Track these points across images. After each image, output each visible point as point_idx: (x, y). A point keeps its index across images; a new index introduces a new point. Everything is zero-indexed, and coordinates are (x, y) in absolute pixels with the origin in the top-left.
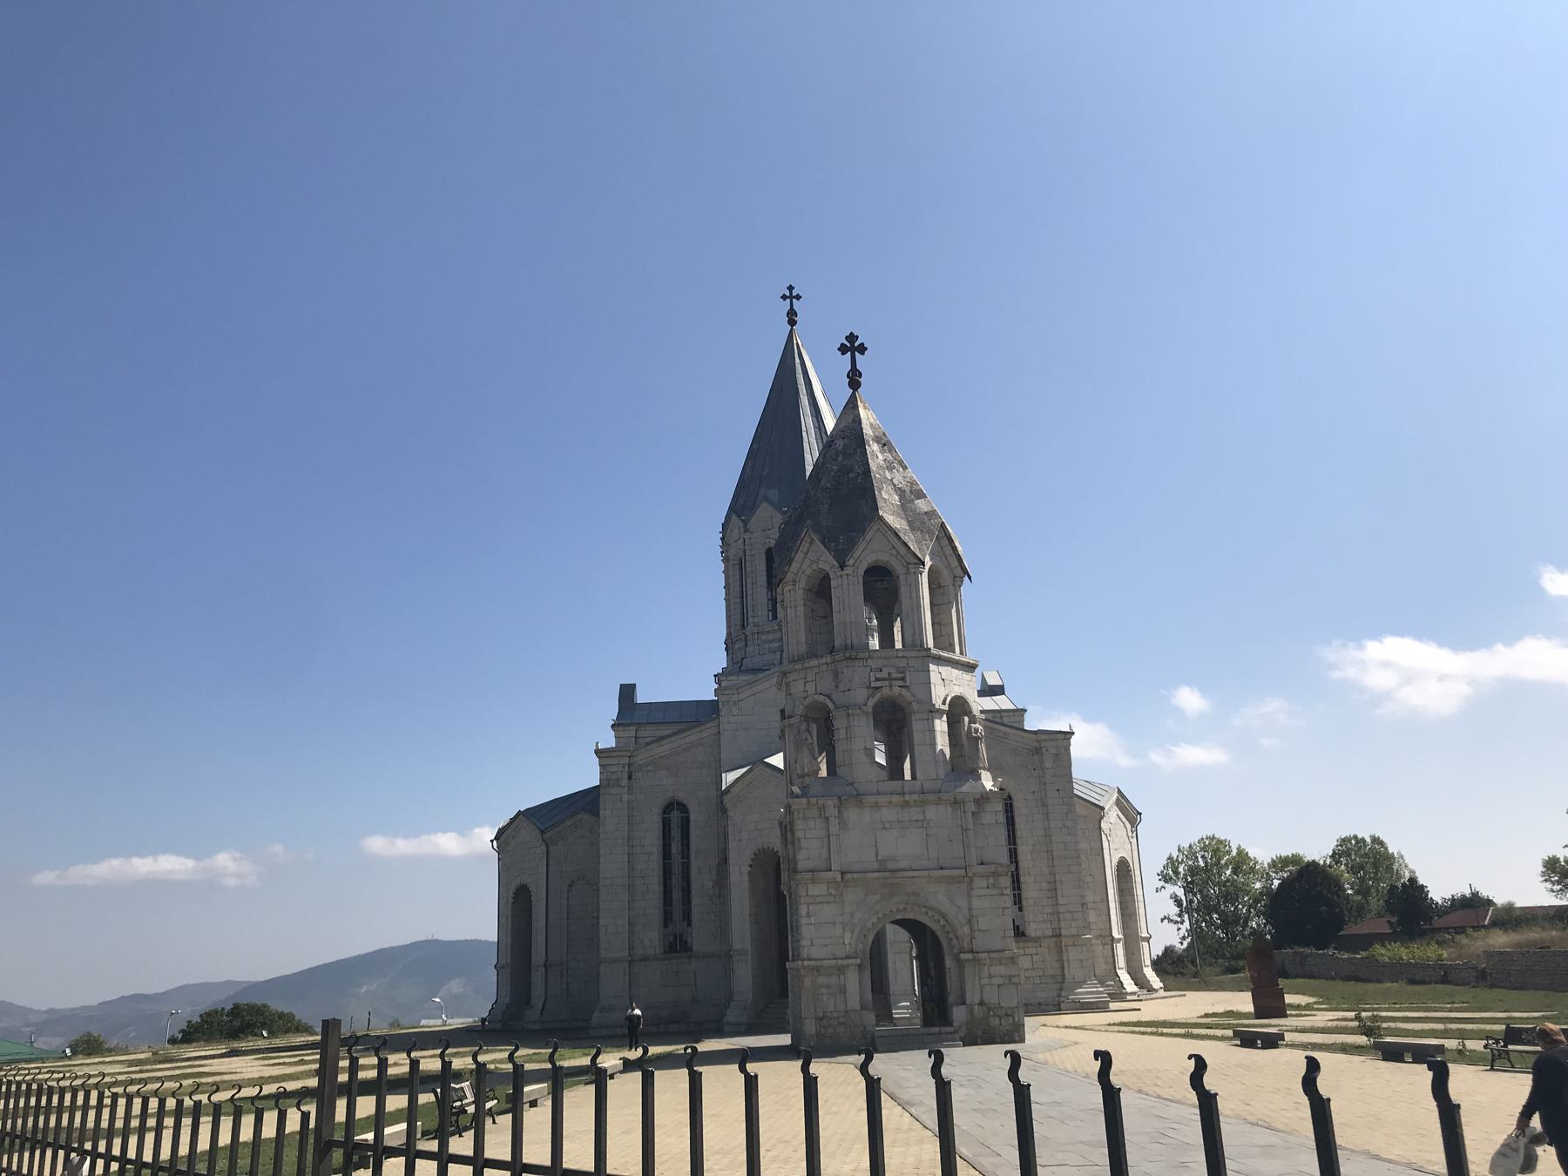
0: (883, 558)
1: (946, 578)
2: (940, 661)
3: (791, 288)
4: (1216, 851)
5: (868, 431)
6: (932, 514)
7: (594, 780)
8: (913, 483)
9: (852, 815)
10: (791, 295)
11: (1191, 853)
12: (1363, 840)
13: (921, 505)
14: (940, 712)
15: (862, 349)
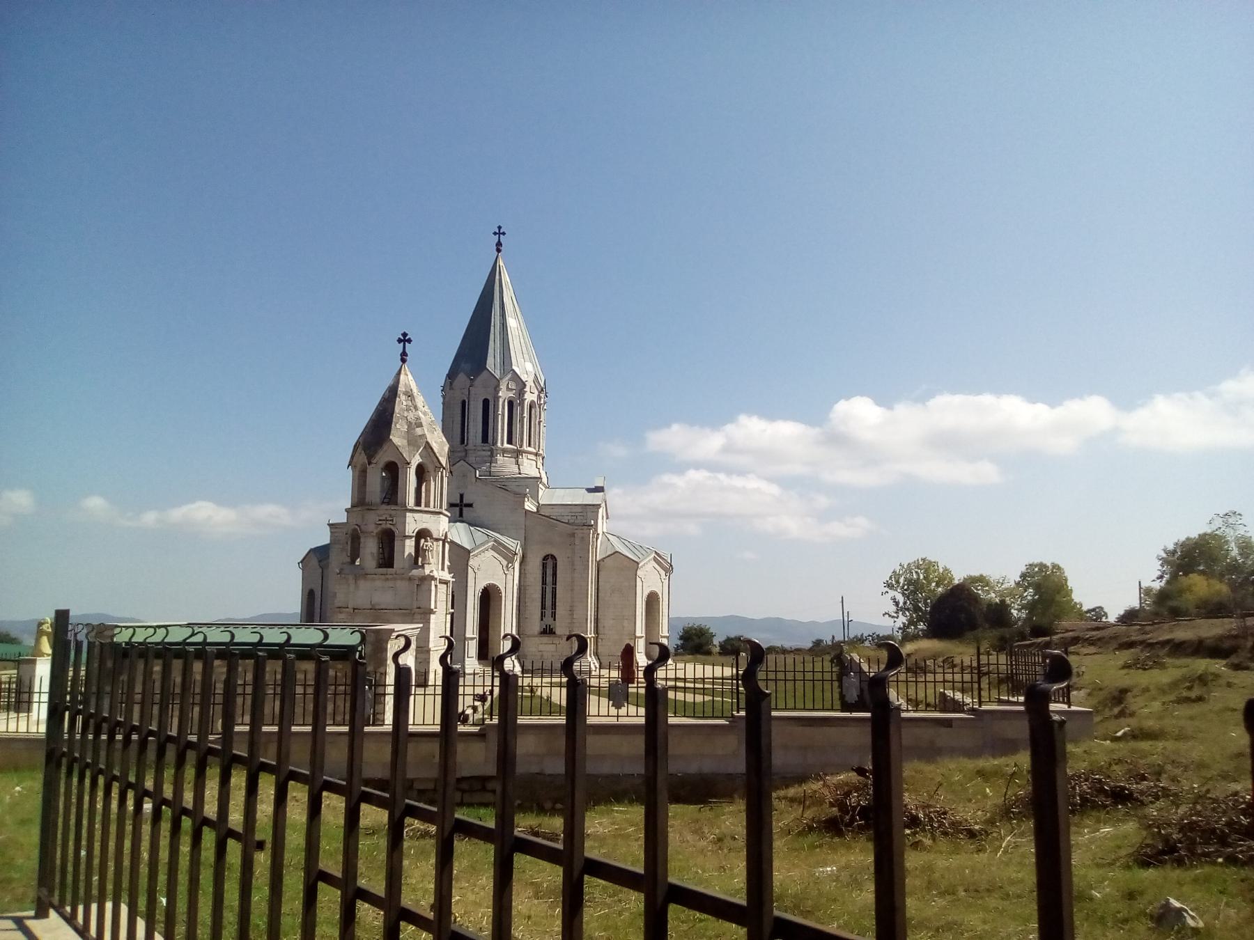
0: (393, 459)
1: (430, 467)
2: (412, 511)
3: (500, 228)
4: (927, 571)
5: (401, 388)
6: (423, 436)
7: (326, 540)
8: (418, 418)
9: (362, 583)
10: (499, 233)
11: (909, 569)
12: (1045, 566)
13: (419, 431)
14: (411, 537)
15: (409, 341)
